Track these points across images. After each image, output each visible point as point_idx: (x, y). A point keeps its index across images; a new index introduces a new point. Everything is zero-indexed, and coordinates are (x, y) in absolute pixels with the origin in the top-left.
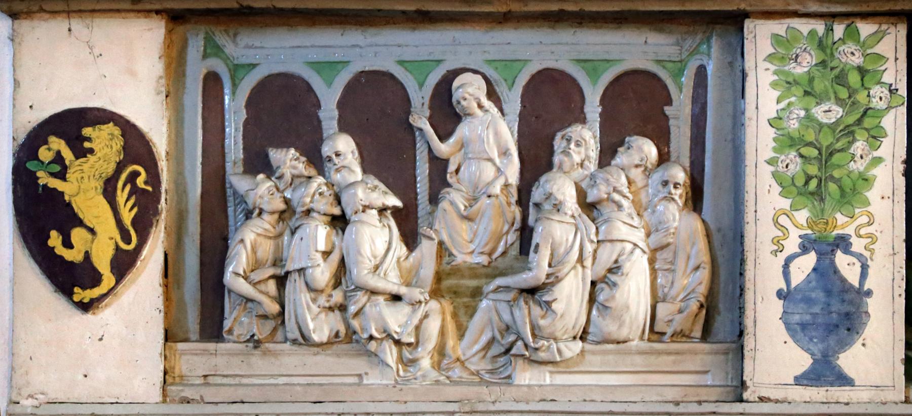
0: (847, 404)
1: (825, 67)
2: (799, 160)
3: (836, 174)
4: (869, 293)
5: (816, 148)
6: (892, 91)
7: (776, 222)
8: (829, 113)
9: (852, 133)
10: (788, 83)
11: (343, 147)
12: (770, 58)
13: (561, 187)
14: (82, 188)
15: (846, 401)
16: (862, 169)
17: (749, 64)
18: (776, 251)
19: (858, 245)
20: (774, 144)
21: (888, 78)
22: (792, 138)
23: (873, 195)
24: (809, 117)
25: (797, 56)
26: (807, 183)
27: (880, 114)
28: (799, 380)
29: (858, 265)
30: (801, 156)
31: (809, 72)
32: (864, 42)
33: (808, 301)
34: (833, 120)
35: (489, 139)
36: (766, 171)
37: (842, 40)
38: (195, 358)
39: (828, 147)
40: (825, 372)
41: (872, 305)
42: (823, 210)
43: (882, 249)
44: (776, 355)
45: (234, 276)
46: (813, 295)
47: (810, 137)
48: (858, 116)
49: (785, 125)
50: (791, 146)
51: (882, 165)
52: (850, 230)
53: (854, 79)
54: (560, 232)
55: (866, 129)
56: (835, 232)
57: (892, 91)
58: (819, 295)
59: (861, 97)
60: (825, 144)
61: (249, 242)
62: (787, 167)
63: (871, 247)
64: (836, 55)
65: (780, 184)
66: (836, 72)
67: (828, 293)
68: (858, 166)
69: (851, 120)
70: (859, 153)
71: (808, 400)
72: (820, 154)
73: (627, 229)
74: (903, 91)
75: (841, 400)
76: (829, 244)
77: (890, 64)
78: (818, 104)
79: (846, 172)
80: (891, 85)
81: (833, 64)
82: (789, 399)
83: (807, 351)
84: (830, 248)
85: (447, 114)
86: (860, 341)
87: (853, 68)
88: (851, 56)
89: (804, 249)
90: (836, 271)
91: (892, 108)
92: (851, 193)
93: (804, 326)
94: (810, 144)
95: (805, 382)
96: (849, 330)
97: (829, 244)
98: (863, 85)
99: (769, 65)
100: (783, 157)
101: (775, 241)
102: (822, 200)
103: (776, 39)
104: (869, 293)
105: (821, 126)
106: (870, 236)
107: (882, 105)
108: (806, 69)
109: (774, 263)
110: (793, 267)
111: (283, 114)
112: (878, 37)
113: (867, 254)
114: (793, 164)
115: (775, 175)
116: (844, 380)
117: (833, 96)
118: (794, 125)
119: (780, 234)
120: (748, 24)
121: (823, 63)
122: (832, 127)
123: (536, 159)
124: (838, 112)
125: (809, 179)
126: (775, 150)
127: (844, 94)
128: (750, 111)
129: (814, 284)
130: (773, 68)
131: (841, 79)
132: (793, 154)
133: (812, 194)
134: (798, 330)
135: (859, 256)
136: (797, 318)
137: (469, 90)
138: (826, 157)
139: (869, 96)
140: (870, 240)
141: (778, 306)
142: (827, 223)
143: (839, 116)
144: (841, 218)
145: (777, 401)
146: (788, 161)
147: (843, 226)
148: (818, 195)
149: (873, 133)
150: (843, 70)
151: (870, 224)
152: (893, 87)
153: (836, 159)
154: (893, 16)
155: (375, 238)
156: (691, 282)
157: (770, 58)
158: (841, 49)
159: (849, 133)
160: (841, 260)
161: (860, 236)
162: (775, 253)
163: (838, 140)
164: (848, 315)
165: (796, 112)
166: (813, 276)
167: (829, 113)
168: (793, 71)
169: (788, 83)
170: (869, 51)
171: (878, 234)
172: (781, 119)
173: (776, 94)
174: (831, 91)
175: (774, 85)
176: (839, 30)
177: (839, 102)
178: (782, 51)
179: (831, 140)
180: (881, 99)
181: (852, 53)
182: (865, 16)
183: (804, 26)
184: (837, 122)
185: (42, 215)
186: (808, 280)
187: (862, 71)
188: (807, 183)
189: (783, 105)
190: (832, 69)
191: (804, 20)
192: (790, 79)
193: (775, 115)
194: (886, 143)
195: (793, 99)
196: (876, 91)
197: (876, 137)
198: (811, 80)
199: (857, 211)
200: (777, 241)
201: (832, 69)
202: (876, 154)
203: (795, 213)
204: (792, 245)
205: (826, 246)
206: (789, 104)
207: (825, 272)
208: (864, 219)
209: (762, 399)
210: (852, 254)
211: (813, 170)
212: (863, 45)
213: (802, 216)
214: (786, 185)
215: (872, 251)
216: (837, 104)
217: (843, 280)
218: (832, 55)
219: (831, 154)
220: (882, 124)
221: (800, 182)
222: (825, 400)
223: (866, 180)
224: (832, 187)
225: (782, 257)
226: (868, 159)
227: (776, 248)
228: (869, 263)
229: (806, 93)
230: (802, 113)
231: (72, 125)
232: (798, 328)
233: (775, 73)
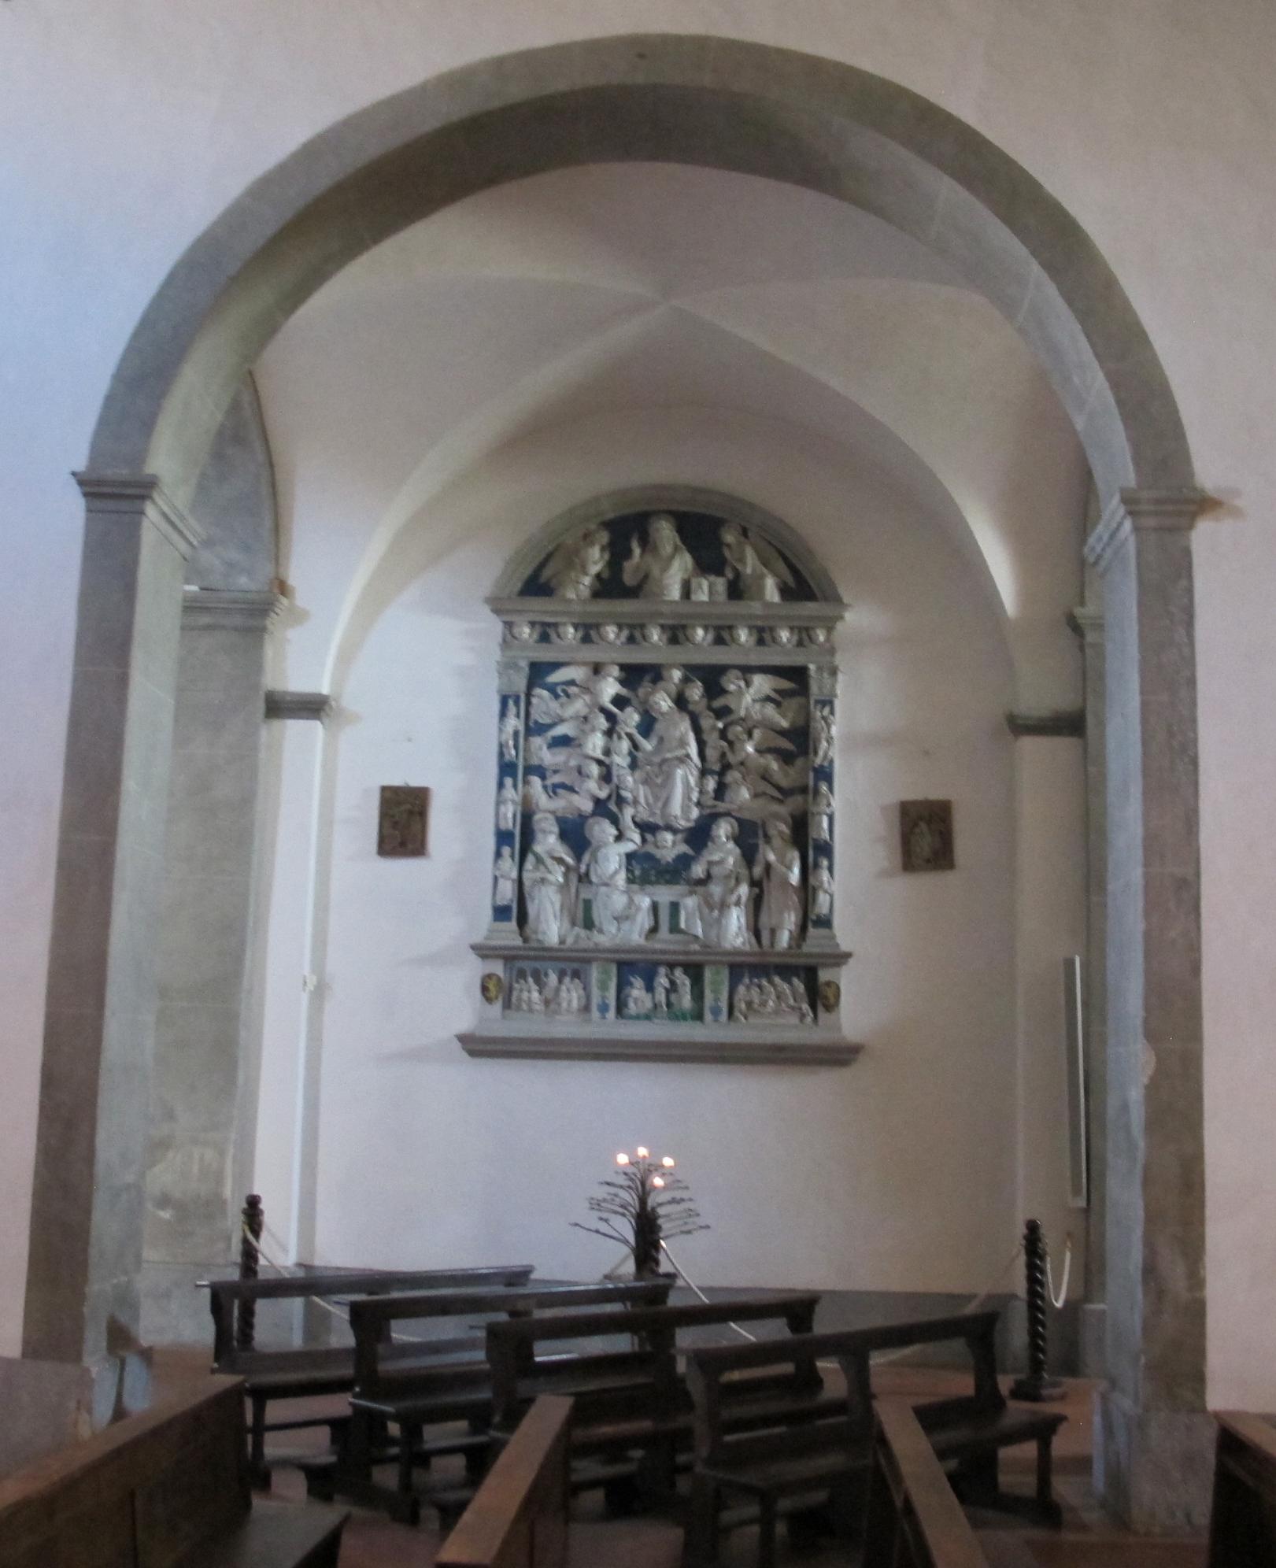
11: (530, 980)
13: (564, 988)
14: (491, 986)
35: (553, 978)
38: (508, 1012)
40: (604, 1018)
44: (595, 1014)
45: (514, 999)
54: (564, 994)
61: (515, 994)
73: (574, 995)
85: (546, 975)
109: (596, 1000)
111: (522, 974)
123: (560, 981)
137: (550, 972)
155: (535, 995)
156: (583, 1001)
185: (484, 989)
205: (603, 998)
231: (489, 976)
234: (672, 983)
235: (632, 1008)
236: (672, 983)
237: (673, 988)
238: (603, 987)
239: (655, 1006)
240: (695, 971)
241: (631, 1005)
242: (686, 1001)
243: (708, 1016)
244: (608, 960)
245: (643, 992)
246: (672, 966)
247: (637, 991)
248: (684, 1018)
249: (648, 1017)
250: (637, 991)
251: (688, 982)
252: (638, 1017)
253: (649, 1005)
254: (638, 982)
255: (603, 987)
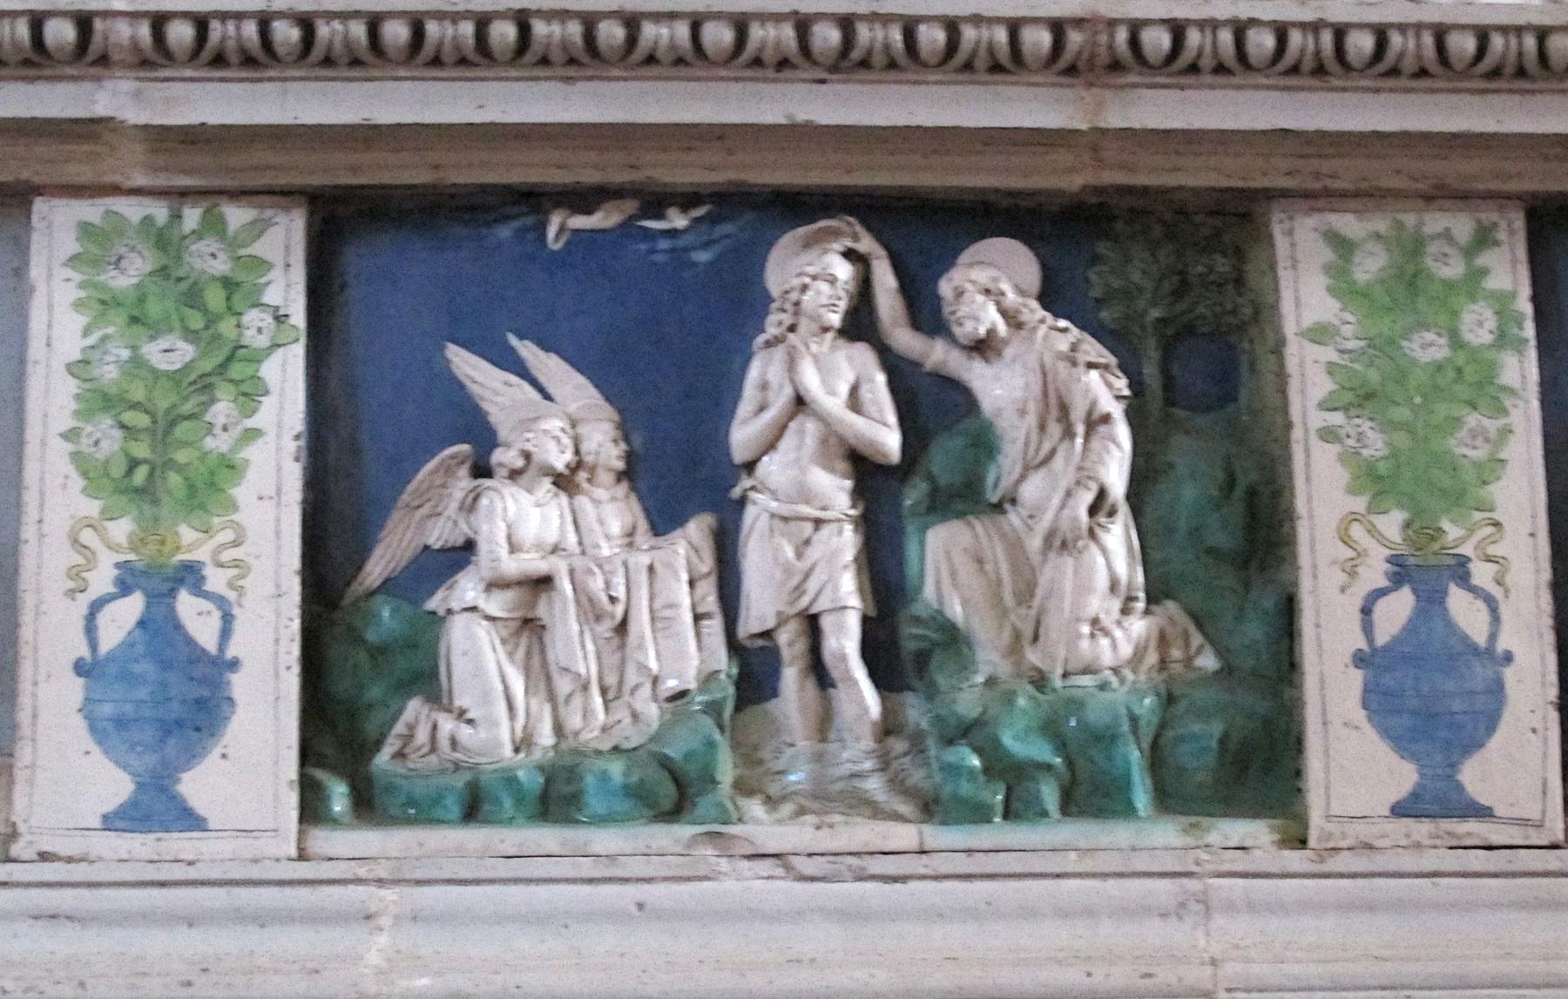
0: (190, 863)
1: (167, 277)
2: (118, 433)
3: (181, 456)
4: (234, 665)
5: (146, 412)
6: (280, 319)
7: (75, 542)
8: (170, 353)
9: (208, 388)
10: (103, 304)
12: (73, 261)
15: (191, 857)
16: (224, 448)
17: (36, 272)
18: (73, 591)
19: (216, 580)
20: (74, 406)
21: (272, 296)
22: (105, 397)
23: (243, 493)
24: (137, 362)
25: (120, 258)
26: (130, 471)
27: (258, 357)
28: (113, 822)
29: (217, 614)
30: (123, 426)
31: (138, 286)
32: (235, 238)
33: (127, 677)
34: (178, 366)
36: (59, 451)
37: (198, 234)
39: (168, 412)
40: (156, 807)
41: (240, 685)
42: (156, 519)
43: (258, 585)
46: (139, 668)
47: (138, 393)
48: (220, 359)
49: (96, 372)
50: (106, 409)
51: (260, 442)
52: (202, 554)
53: (215, 298)
55: (231, 381)
56: (180, 557)
57: (280, 319)
58: (145, 668)
59: (226, 327)
60: (163, 404)
62: (96, 443)
63: (240, 583)
64: (187, 258)
65: (85, 474)
66: (184, 286)
67: (166, 665)
68: (218, 443)
69: (208, 365)
70: (221, 420)
71: (125, 856)
72: (154, 422)
74: (299, 318)
75: (182, 857)
76: (167, 579)
77: (276, 274)
78: (153, 338)
79: (197, 454)
80: (277, 308)
81: (181, 273)
82: (92, 857)
83: (125, 767)
84: (169, 585)
86: (217, 752)
87: (214, 278)
88: (207, 259)
89: (124, 587)
90: (178, 626)
91: (279, 346)
92: (209, 488)
93: (121, 723)
94: (135, 406)
95: (121, 824)
96: (198, 729)
97: (167, 579)
98: (229, 308)
99: (70, 273)
100: (89, 428)
101: (74, 571)
102: (155, 502)
103: (85, 230)
104: (234, 665)
105: (155, 372)
106: (236, 563)
107: (263, 341)
108: (135, 281)
110: (103, 618)
112: (258, 229)
113: (232, 596)
114: (106, 439)
115: (76, 457)
116: (191, 821)
117: (177, 325)
118: (109, 373)
119: (80, 560)
120: (40, 206)
121: (162, 272)
122: (175, 377)
124: (185, 351)
125: (133, 464)
126: (77, 414)
127: (196, 321)
128: (36, 349)
129: (140, 649)
130: (78, 277)
131: (193, 297)
132: (107, 422)
133: (139, 491)
134: (107, 730)
135: (220, 601)
136: (107, 709)
138: (165, 428)
139: (239, 326)
140: (235, 571)
141: (76, 688)
142: (163, 543)
143: (188, 359)
144: (187, 534)
145: (70, 860)
146: (99, 435)
147: (192, 547)
148: (146, 494)
149: (244, 388)
150: (196, 283)
151: (236, 544)
152: (281, 312)
153: (181, 431)
154: (284, 195)
157: (73, 261)
158: (193, 248)
159: (205, 387)
160: (187, 605)
161: (221, 565)
162: (71, 594)
163: (186, 399)
164: (200, 704)
165: (114, 351)
166: (137, 633)
167: (170, 353)
168: (112, 283)
169: (103, 302)
170: (242, 252)
171: (250, 560)
172: (88, 363)
173: (82, 320)
174: (174, 317)
175: (78, 305)
176: (192, 216)
177: (190, 335)
178: (94, 250)
179: (174, 398)
180: (260, 330)
181: (213, 255)
182: (239, 194)
183: (132, 210)
184: (187, 367)
186: (128, 644)
187: (229, 284)
188: (130, 471)
189: (92, 340)
190: (179, 280)
191: (133, 200)
192: (106, 297)
193: (77, 356)
194: (268, 405)
195: (110, 330)
196: (253, 317)
197: (251, 394)
198: (141, 300)
199: (216, 520)
200: (75, 573)
201: (179, 280)
202: (250, 423)
203: (109, 524)
204: (102, 579)
205: (161, 581)
206: (104, 339)
207: (159, 628)
208: (227, 536)
209: (44, 857)
210: (207, 596)
211: (141, 450)
212: (232, 244)
213: (121, 529)
214: (92, 473)
215: (240, 590)
216: (186, 340)
217: (190, 642)
218: (179, 258)
219: (173, 423)
220: (259, 374)
221: (118, 470)
222: (155, 857)
223: (231, 467)
224: (174, 479)
225: (84, 601)
226: (236, 432)
227: (71, 584)
228: (236, 611)
229: (134, 320)
230: (125, 354)
232: (110, 726)
233: (82, 286)
234: (930, 403)
235: (489, 698)
236: (930, 403)
237: (929, 465)
238: (159, 468)
239: (754, 672)
240: (1166, 267)
241: (477, 651)
242: (1101, 615)
243: (1351, 763)
244: (209, 167)
245: (611, 512)
246: (920, 225)
247: (541, 497)
248: (1090, 794)
249: (672, 791)
250: (541, 497)
251: (1103, 390)
252: (556, 796)
253: (686, 655)
254: (552, 410)
255: (159, 468)
